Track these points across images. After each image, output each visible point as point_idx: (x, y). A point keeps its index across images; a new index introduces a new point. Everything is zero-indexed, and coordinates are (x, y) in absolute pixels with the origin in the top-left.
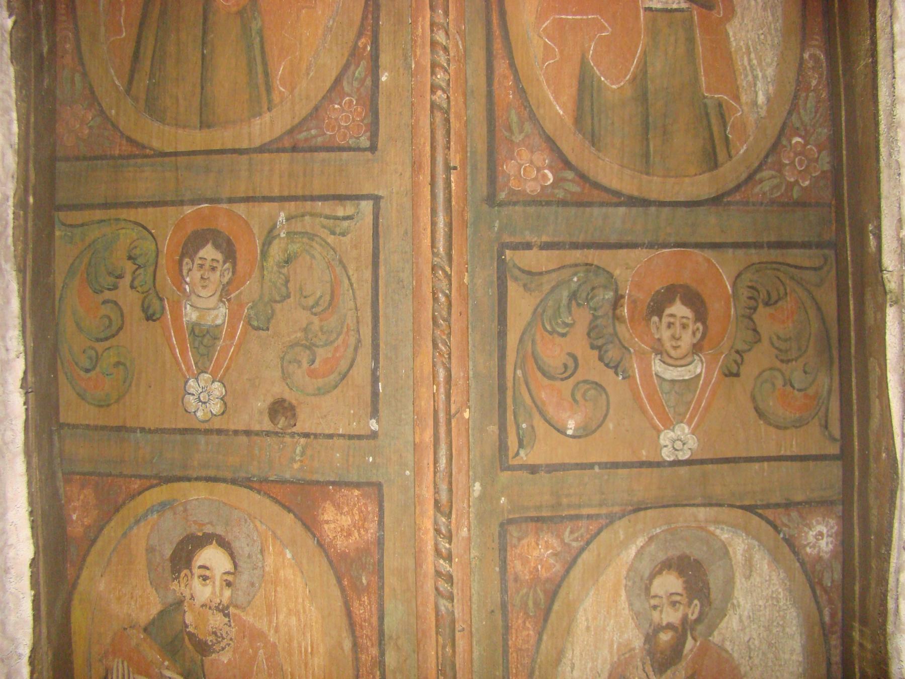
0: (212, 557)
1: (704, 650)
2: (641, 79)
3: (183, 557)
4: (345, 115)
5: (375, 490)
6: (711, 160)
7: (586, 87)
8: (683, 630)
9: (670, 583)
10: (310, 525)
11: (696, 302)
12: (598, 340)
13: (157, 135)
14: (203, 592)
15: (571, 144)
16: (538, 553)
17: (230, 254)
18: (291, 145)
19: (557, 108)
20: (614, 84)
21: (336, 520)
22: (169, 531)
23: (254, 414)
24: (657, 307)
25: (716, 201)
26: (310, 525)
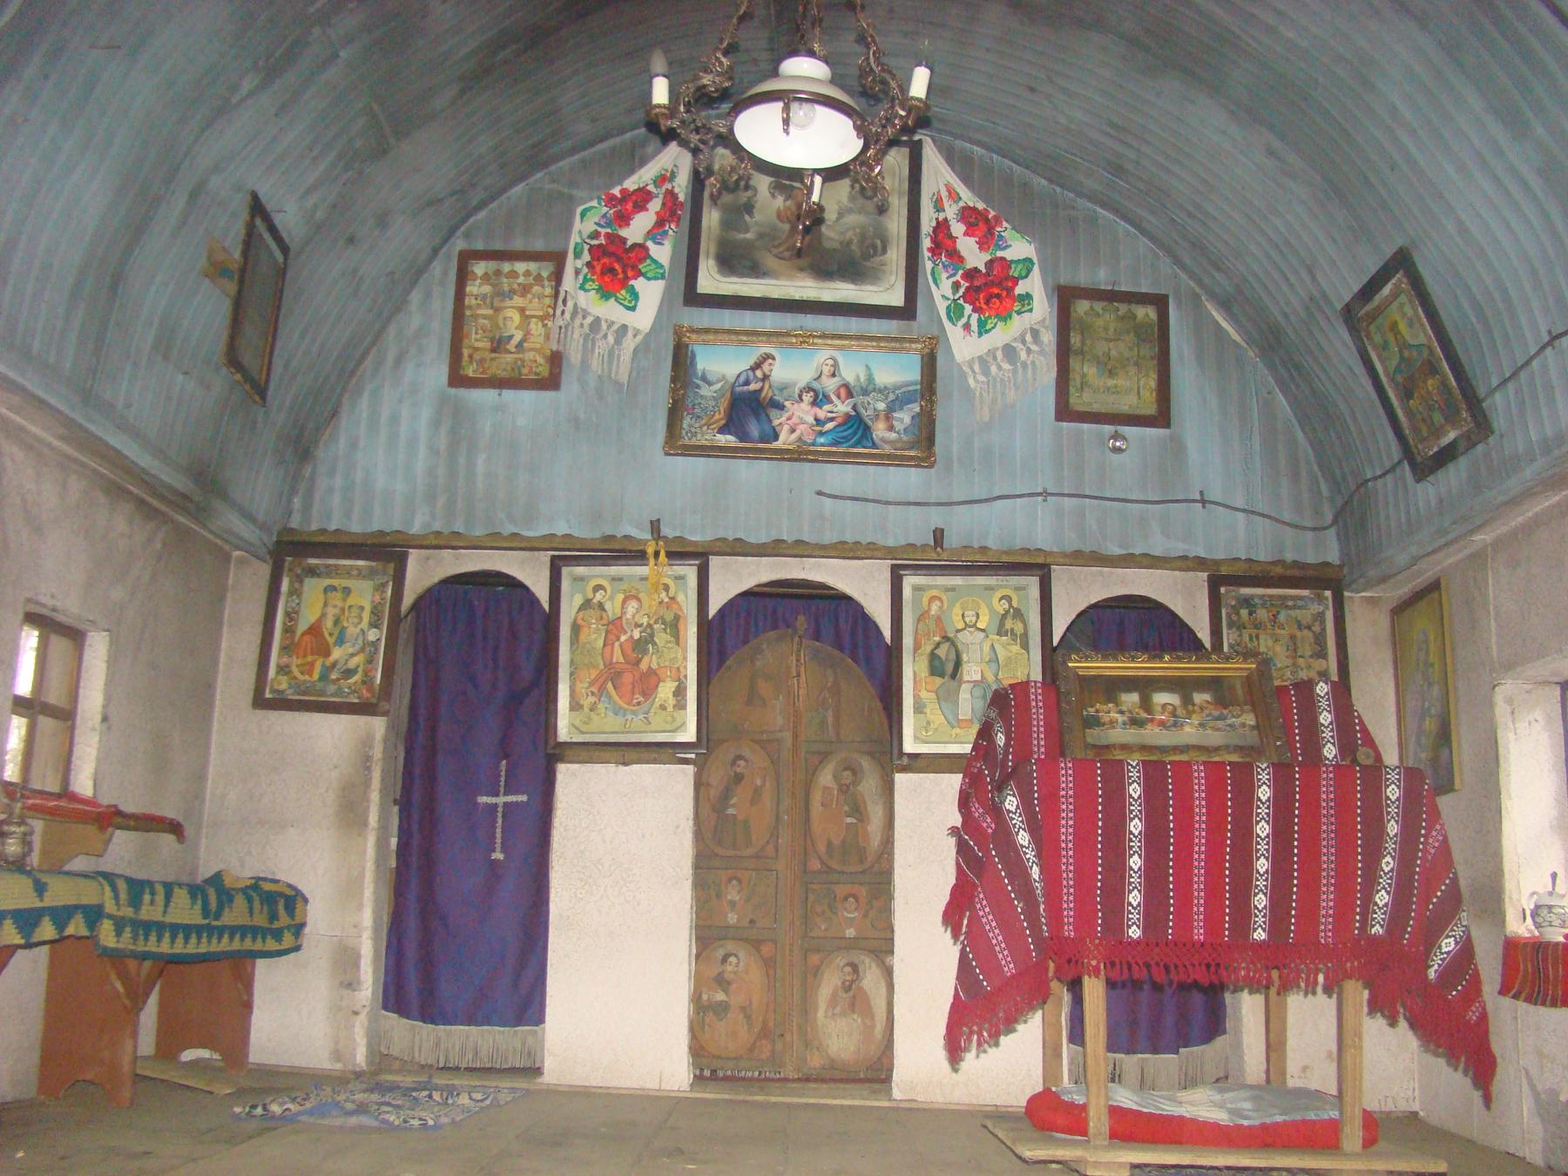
0: (732, 959)
1: (861, 989)
2: (844, 841)
3: (724, 960)
4: (770, 849)
5: (775, 942)
6: (861, 861)
7: (829, 844)
8: (852, 981)
9: (848, 969)
10: (758, 951)
11: (854, 896)
12: (830, 907)
13: (720, 851)
14: (729, 968)
15: (824, 857)
16: (814, 959)
17: (740, 882)
18: (757, 856)
19: (822, 848)
20: (836, 842)
21: (766, 950)
22: (720, 953)
23: (745, 923)
24: (846, 899)
25: (863, 872)
26: (758, 951)
